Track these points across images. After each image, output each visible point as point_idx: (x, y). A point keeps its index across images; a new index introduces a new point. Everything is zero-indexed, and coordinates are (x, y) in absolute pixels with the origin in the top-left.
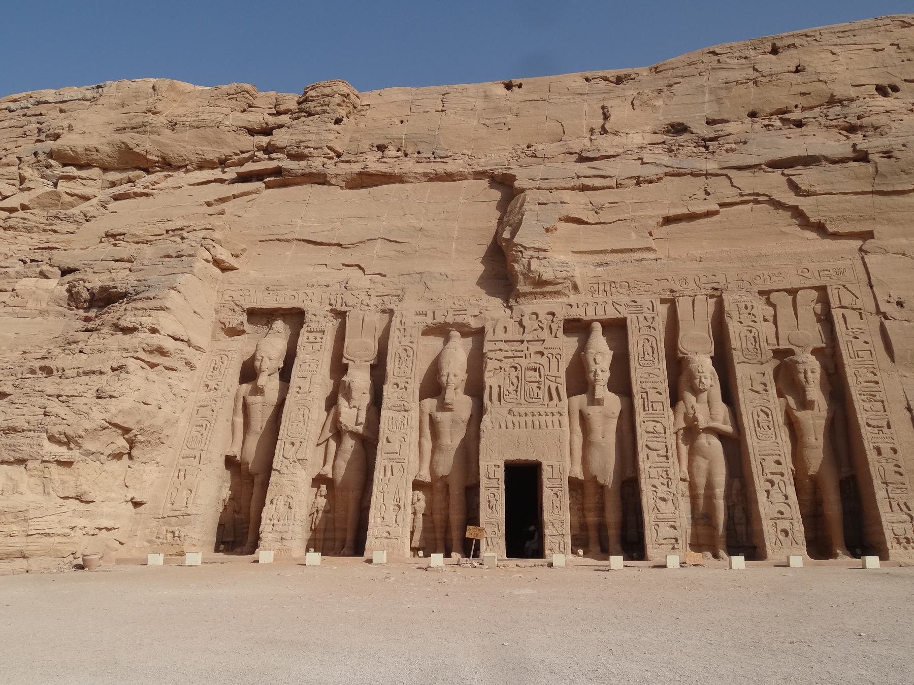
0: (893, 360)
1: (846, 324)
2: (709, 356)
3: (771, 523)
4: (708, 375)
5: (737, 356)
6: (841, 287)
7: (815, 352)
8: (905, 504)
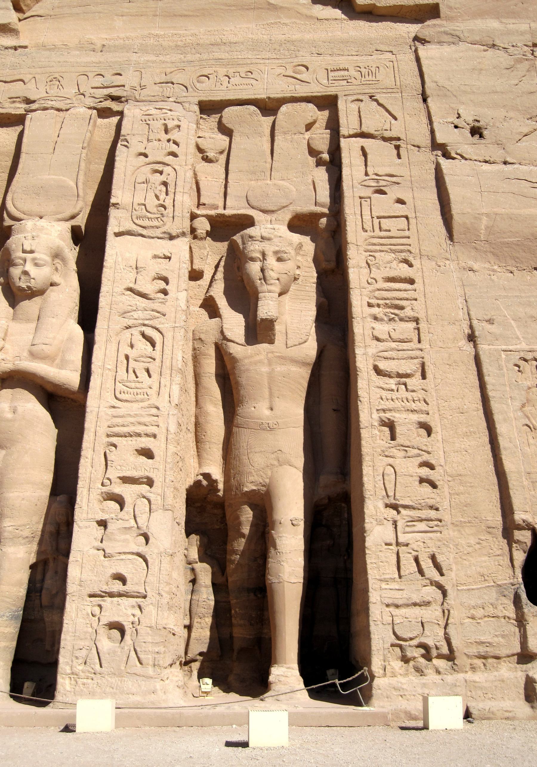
0: (451, 237)
1: (366, 165)
2: (68, 225)
3: (90, 605)
4: (42, 256)
5: (116, 220)
6: (366, 98)
7: (300, 224)
8: (433, 558)
